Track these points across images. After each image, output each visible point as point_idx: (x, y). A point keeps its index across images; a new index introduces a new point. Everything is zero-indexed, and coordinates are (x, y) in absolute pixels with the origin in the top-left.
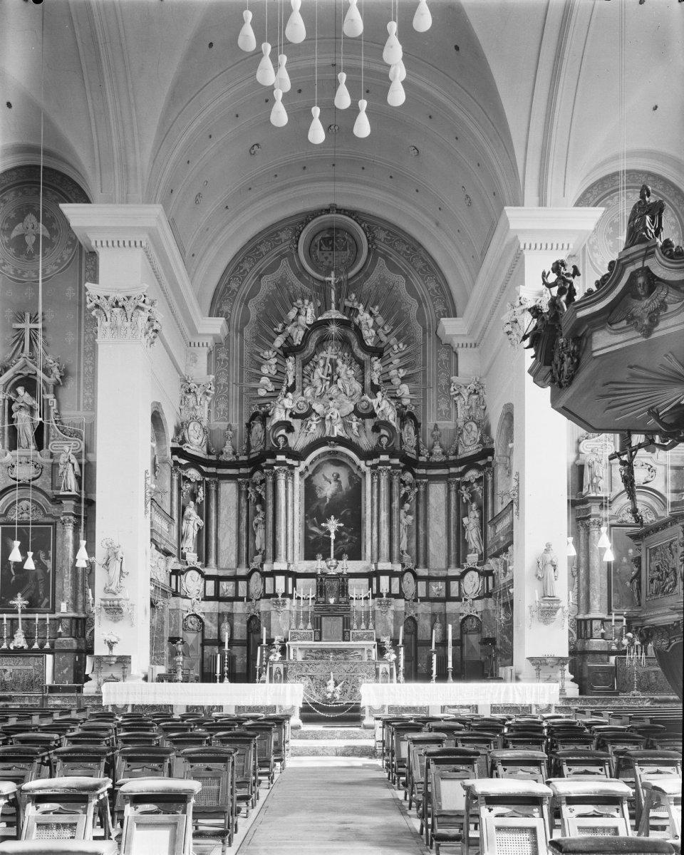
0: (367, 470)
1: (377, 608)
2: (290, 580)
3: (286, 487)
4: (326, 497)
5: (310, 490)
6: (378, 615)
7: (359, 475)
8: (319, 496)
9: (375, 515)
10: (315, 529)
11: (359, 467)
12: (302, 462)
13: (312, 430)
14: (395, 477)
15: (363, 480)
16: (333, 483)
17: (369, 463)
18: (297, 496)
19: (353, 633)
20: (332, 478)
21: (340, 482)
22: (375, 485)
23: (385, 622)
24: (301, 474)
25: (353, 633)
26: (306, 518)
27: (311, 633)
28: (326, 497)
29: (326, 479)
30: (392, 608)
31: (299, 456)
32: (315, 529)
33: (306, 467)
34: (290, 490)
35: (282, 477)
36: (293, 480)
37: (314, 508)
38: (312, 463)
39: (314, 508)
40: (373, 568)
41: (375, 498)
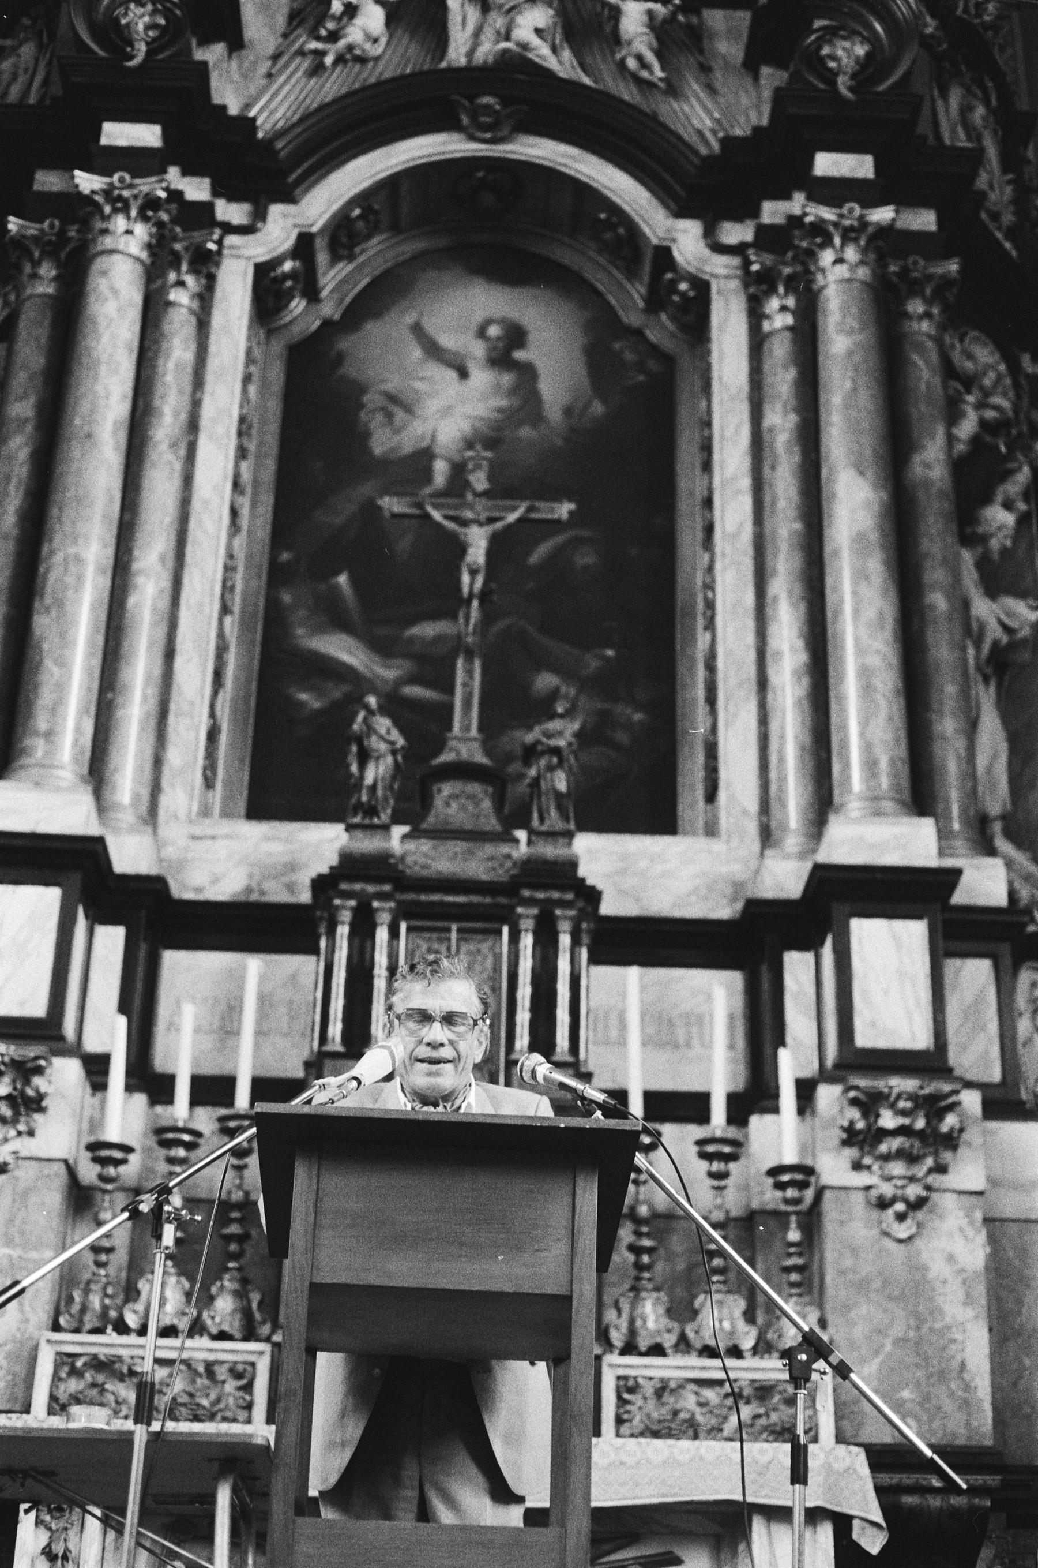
0: (720, 269)
1: (834, 1168)
2: (111, 940)
3: (153, 310)
4: (425, 456)
5: (316, 417)
6: (852, 1234)
7: (661, 331)
8: (381, 442)
9: (786, 526)
10: (344, 650)
11: (664, 255)
12: (276, 210)
13: (354, 34)
14: (916, 306)
15: (685, 363)
16: (481, 378)
17: (735, 233)
18: (224, 402)
19: (627, 1387)
20: (478, 349)
21: (527, 373)
22: (780, 349)
23: (914, 1292)
24: (269, 291)
25: (627, 1387)
26: (277, 575)
27: (244, 1375)
28: (425, 456)
29: (433, 351)
30: (967, 1172)
31: (260, 170)
32: (344, 650)
33: (304, 245)
34: (178, 351)
35: (127, 240)
36: (205, 299)
37: (340, 512)
38: (343, 234)
39: (340, 512)
40: (785, 878)
41: (781, 421)
